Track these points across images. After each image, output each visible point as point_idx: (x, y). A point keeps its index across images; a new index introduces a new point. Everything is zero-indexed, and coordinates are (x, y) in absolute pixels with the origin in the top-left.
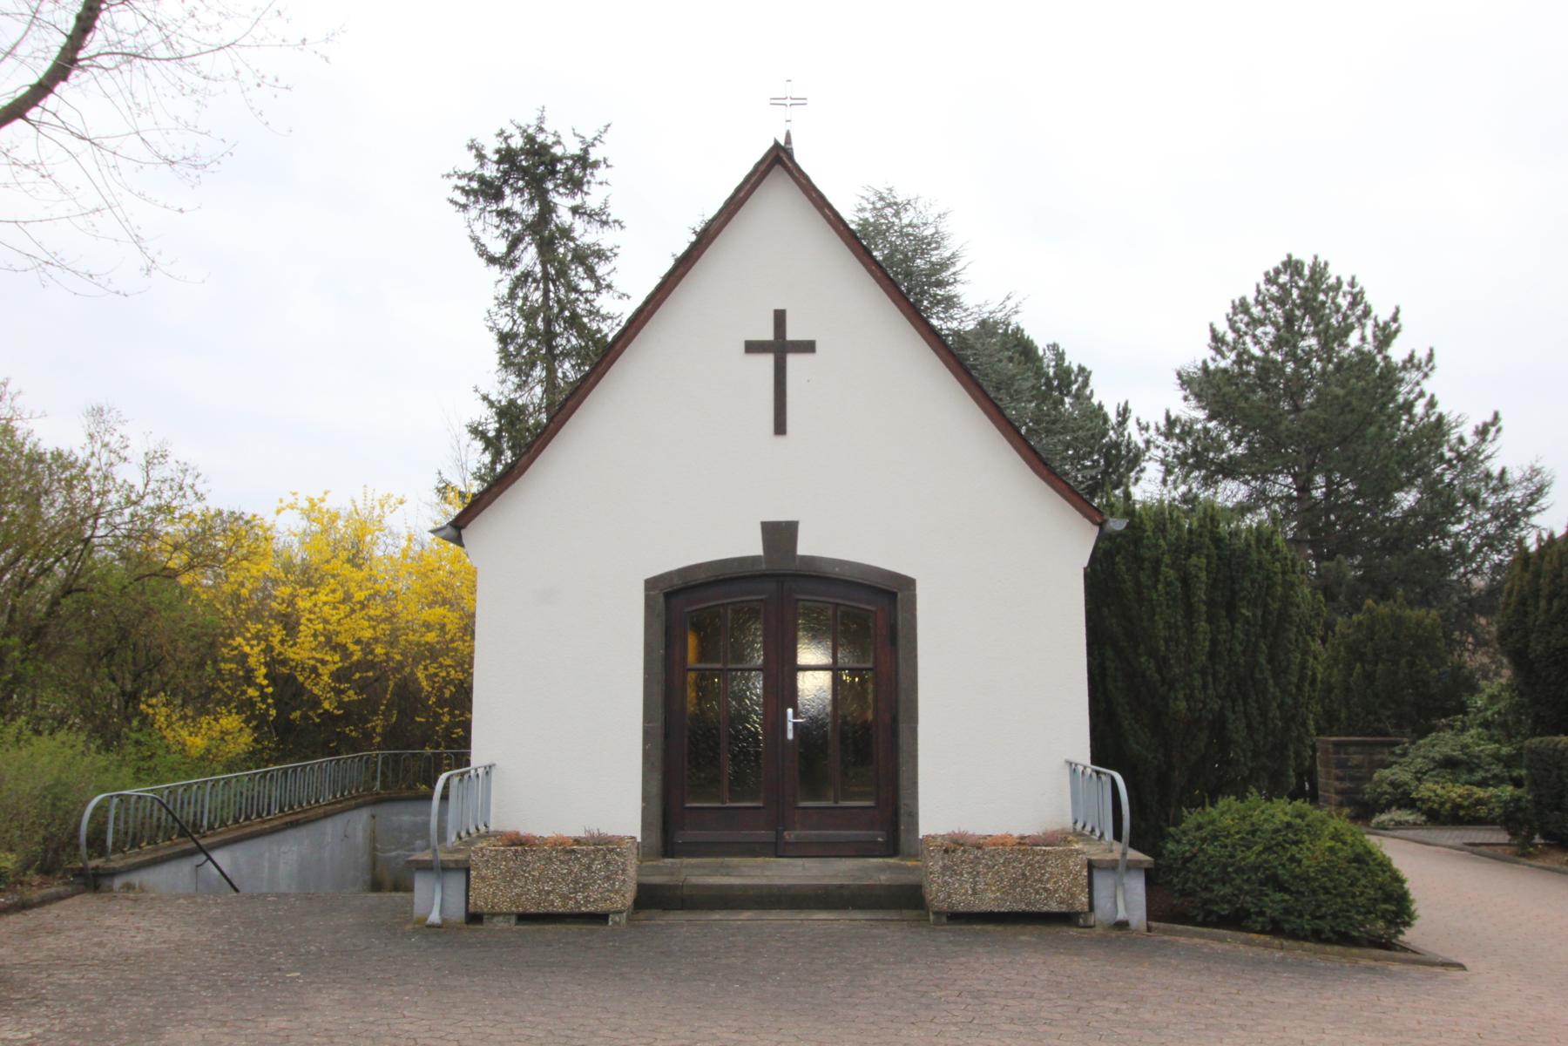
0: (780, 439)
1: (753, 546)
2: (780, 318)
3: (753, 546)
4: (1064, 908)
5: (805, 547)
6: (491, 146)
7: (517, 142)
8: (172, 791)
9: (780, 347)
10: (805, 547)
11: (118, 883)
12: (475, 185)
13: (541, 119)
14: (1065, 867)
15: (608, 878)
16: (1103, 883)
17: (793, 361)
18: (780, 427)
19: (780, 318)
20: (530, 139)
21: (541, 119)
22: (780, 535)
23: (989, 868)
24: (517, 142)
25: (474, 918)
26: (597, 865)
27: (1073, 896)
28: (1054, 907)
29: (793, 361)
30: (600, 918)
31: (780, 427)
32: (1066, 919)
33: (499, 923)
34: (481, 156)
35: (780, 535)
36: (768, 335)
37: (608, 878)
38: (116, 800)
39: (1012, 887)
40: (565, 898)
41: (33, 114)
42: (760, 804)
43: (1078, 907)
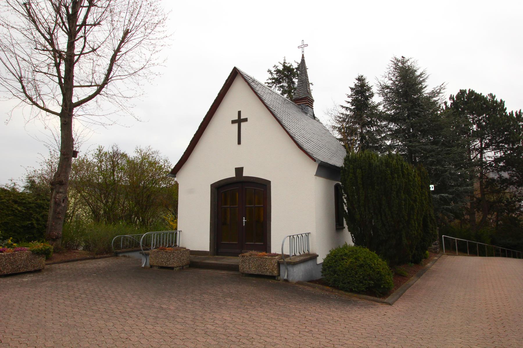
0: (239, 145)
1: (233, 175)
2: (239, 113)
3: (233, 175)
4: (271, 274)
5: (244, 174)
6: (273, 69)
7: (281, 68)
8: (133, 236)
9: (239, 121)
10: (244, 174)
11: (121, 255)
12: (274, 81)
13: (285, 60)
14: (271, 263)
15: (173, 259)
16: (282, 268)
17: (243, 124)
18: (239, 143)
19: (239, 113)
20: (284, 66)
21: (285, 60)
22: (239, 171)
23: (253, 262)
24: (281, 68)
25: (151, 266)
26: (171, 256)
27: (273, 271)
28: (268, 274)
29: (243, 124)
30: (172, 268)
31: (239, 143)
32: (273, 277)
33: (155, 268)
34: (271, 73)
35: (239, 171)
36: (236, 118)
37: (173, 259)
38: (122, 238)
39: (258, 267)
40: (165, 263)
41: (101, 92)
42: (262, 244)
43: (274, 275)
